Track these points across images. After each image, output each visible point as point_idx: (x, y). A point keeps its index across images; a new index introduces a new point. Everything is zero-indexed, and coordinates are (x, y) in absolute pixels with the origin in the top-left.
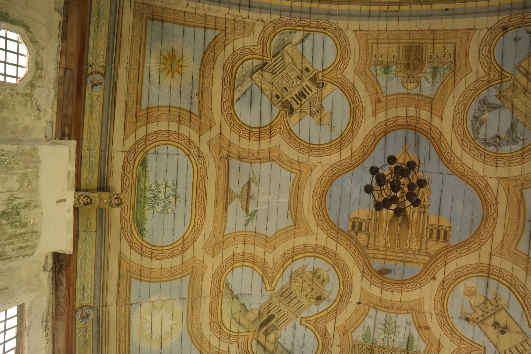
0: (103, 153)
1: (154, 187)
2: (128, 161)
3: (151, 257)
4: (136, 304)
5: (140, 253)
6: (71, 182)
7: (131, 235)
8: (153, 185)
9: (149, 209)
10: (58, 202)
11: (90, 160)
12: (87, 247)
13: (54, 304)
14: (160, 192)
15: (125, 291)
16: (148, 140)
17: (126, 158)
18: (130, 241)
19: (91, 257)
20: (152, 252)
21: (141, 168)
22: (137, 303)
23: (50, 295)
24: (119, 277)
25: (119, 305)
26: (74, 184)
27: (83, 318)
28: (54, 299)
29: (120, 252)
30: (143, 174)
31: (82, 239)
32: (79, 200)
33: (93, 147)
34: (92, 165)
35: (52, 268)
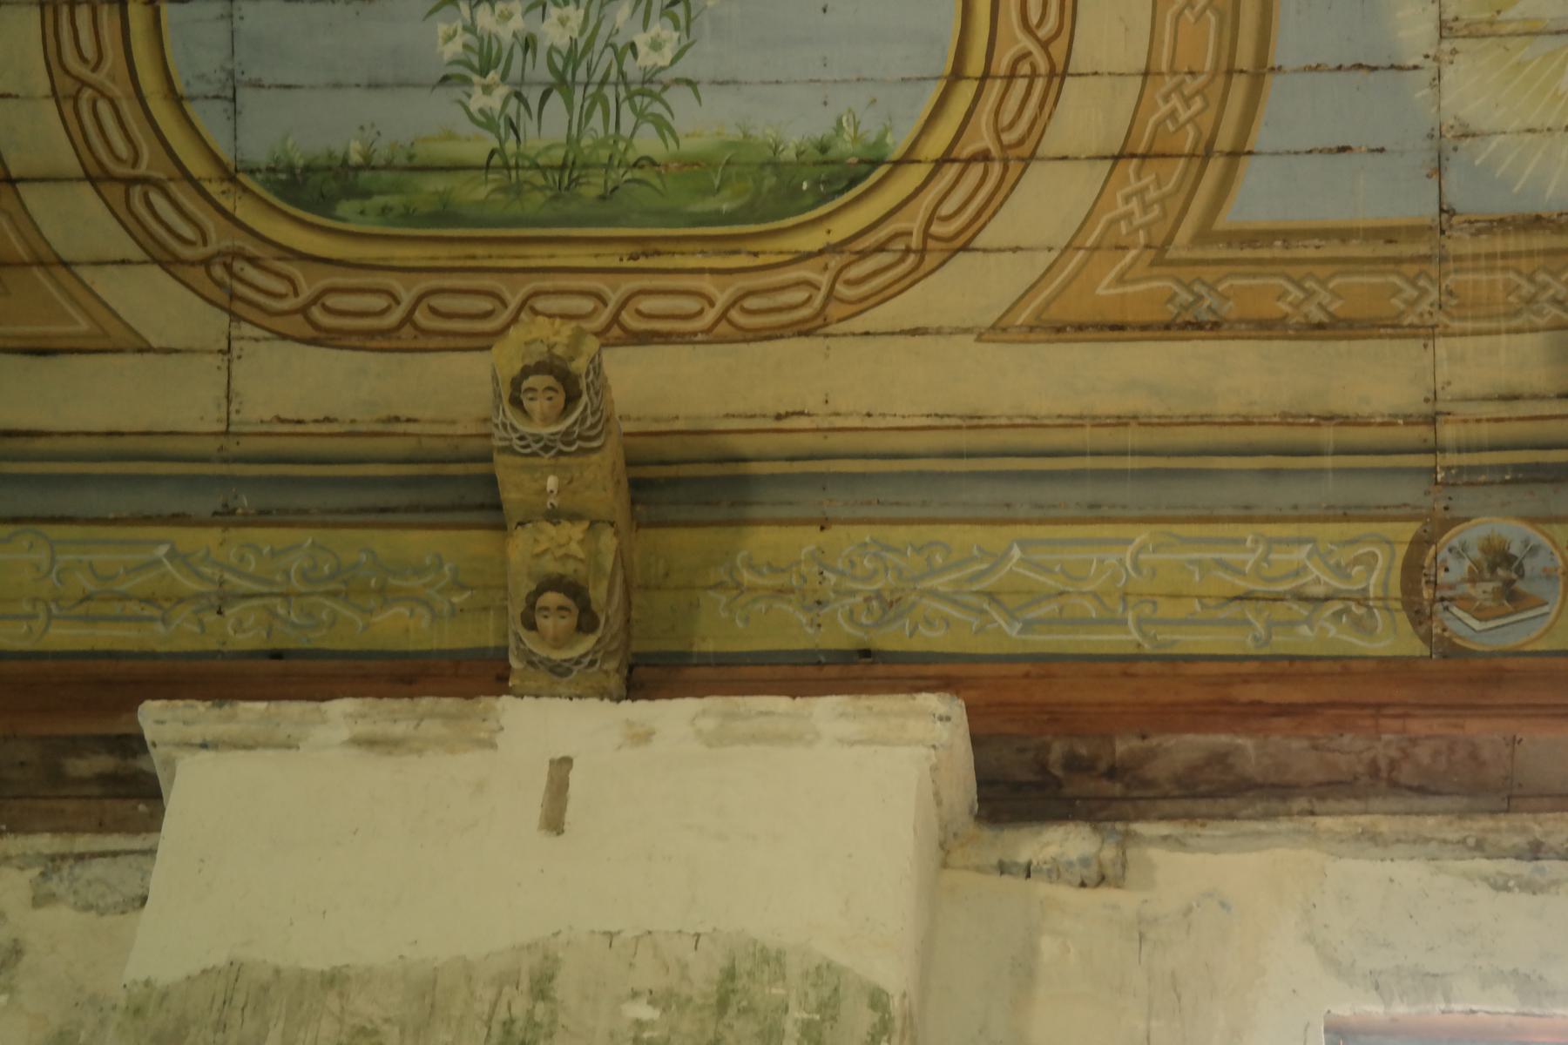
0: (244, 502)
1: (487, 90)
2: (303, 310)
3: (1052, 73)
4: (1452, 178)
5: (1015, 168)
6: (433, 728)
7: (863, 255)
8: (478, 101)
9: (662, 127)
10: (554, 822)
11: (297, 585)
12: (940, 583)
13: (1394, 803)
14: (529, 44)
15: (1321, 271)
16: (135, 162)
17: (280, 324)
18: (912, 259)
19: (1016, 553)
20: (1011, 76)
21: (346, 208)
22: (1439, 171)
23: (1314, 836)
24: (1199, 326)
25: (1441, 318)
26: (448, 704)
27: (1511, 596)
28: (1357, 805)
29: (998, 331)
30: (396, 188)
31: (878, 624)
32: (559, 670)
33: (199, 576)
34: (332, 577)
35: (1095, 829)
